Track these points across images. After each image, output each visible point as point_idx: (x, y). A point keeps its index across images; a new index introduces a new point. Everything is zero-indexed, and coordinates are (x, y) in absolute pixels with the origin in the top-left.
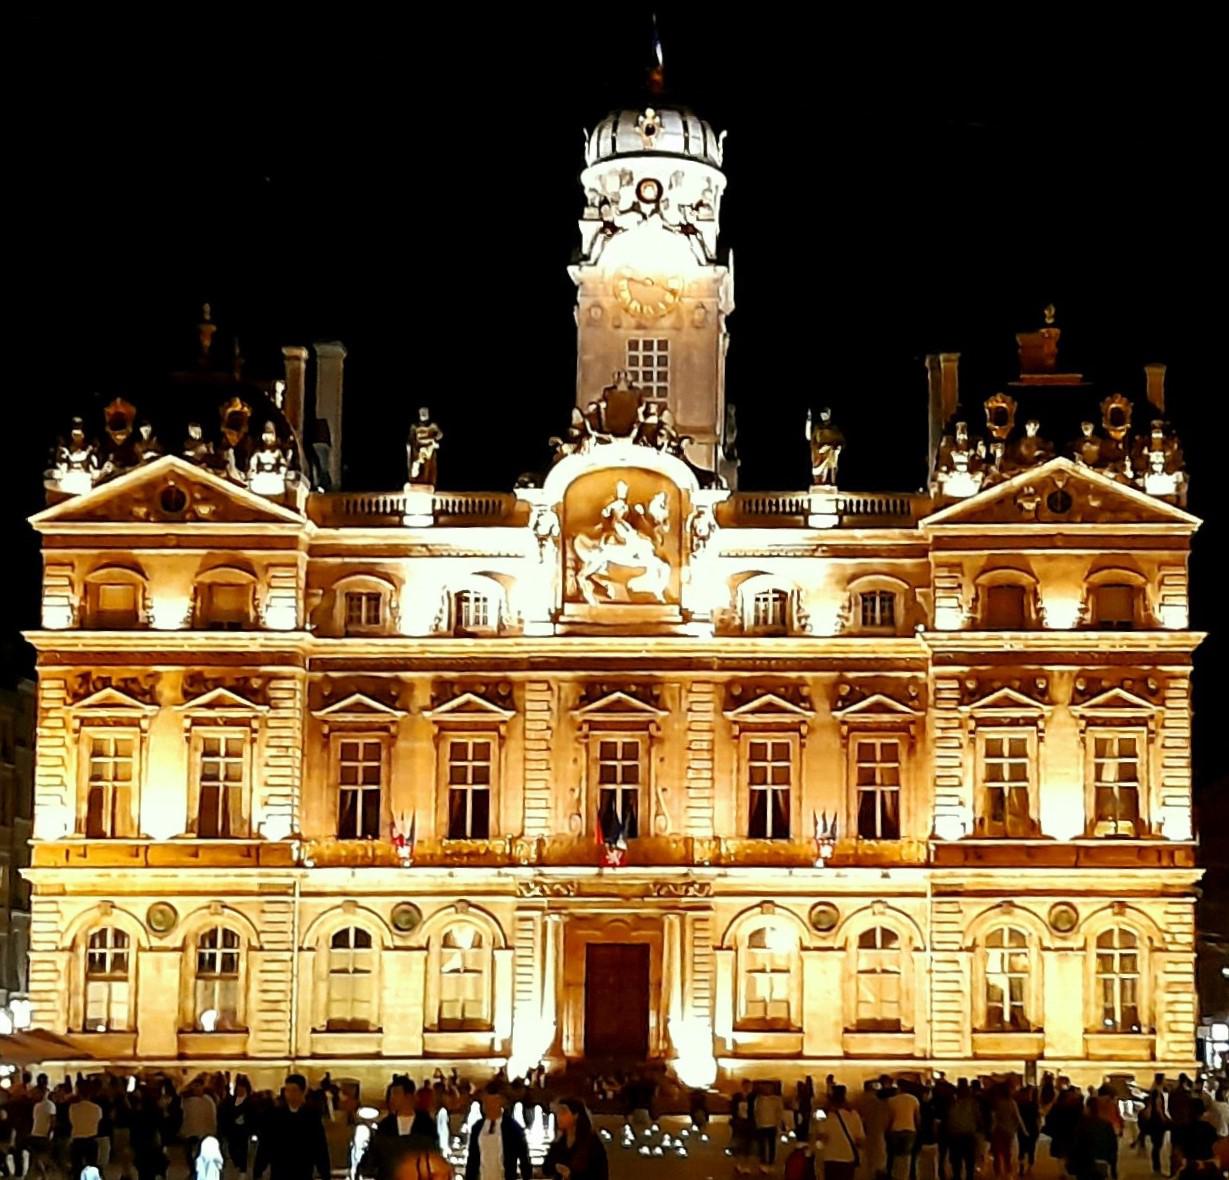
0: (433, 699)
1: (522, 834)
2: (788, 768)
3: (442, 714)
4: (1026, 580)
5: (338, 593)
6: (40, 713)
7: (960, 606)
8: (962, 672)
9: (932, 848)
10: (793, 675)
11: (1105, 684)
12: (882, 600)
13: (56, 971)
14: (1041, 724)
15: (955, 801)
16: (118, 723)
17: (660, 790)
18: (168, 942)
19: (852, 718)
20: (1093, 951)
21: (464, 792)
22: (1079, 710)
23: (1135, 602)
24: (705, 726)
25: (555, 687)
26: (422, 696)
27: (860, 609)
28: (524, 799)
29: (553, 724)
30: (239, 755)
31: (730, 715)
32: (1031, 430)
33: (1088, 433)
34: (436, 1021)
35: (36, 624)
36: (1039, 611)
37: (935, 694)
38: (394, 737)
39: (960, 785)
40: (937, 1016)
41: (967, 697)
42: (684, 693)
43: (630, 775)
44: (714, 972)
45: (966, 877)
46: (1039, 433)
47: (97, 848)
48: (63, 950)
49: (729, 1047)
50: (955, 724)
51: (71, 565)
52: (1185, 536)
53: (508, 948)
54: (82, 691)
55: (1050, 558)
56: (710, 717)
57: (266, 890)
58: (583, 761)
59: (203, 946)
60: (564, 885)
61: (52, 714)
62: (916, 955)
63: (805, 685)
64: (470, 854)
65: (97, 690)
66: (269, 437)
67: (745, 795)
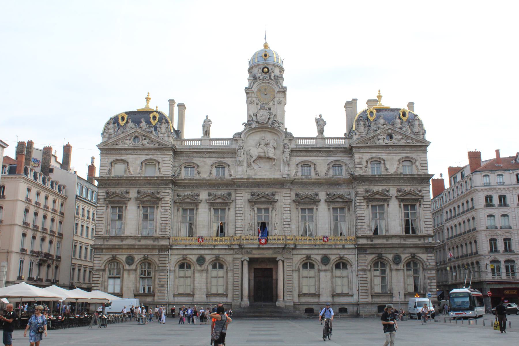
24: (288, 203)
40: (360, 288)
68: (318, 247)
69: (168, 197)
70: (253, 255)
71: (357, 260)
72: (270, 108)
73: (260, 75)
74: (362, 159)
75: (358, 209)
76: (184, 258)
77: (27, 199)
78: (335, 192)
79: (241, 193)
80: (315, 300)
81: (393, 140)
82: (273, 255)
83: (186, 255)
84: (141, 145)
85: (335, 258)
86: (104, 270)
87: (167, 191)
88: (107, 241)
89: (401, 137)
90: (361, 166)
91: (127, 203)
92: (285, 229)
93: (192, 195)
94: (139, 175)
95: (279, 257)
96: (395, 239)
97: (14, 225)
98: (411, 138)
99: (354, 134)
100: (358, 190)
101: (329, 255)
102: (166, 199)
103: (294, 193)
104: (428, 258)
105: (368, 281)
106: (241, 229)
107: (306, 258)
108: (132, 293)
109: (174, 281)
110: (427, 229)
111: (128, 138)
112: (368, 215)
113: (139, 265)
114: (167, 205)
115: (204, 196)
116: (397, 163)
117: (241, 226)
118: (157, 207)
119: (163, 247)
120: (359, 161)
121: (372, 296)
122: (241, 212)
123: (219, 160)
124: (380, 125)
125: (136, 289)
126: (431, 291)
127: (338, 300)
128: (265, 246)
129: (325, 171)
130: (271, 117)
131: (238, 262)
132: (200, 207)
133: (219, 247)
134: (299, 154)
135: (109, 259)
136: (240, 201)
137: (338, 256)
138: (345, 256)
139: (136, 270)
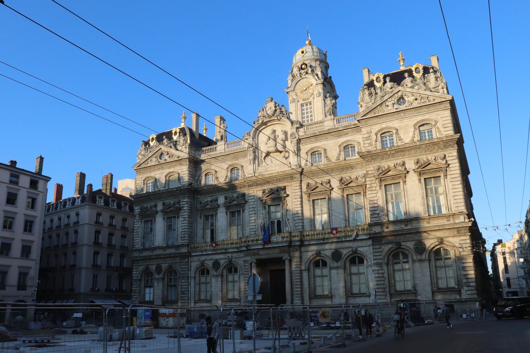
68: (327, 241)
69: (186, 205)
70: (259, 256)
72: (310, 103)
73: (297, 72)
74: (371, 132)
76: (203, 263)
77: (97, 222)
78: (348, 176)
79: (253, 192)
80: (328, 302)
81: (406, 104)
82: (280, 254)
83: (204, 261)
84: (164, 160)
85: (347, 253)
86: (140, 280)
87: (186, 200)
88: (142, 253)
89: (413, 98)
90: (369, 141)
91: (155, 216)
92: (297, 225)
93: (211, 201)
94: (164, 189)
95: (285, 256)
96: (416, 223)
97: (83, 245)
98: (427, 96)
99: (359, 106)
100: (368, 169)
101: (340, 250)
102: (185, 208)
103: (305, 184)
104: (461, 242)
105: (385, 278)
106: (254, 230)
107: (315, 255)
108: (161, 300)
109: (195, 288)
110: (457, 206)
111: (154, 156)
112: (381, 198)
113: (166, 274)
114: (186, 213)
115: (221, 200)
116: (413, 130)
117: (254, 227)
118: (178, 217)
119: (182, 255)
120: (367, 136)
121: (391, 295)
122: (254, 212)
123: (234, 162)
124: (388, 90)
127: (352, 301)
128: (270, 246)
129: (337, 155)
130: (277, 109)
131: (247, 264)
132: (218, 212)
133: (230, 251)
134: (309, 140)
135: (143, 270)
136: (252, 200)
137: (350, 249)
138: (359, 249)
139: (163, 279)
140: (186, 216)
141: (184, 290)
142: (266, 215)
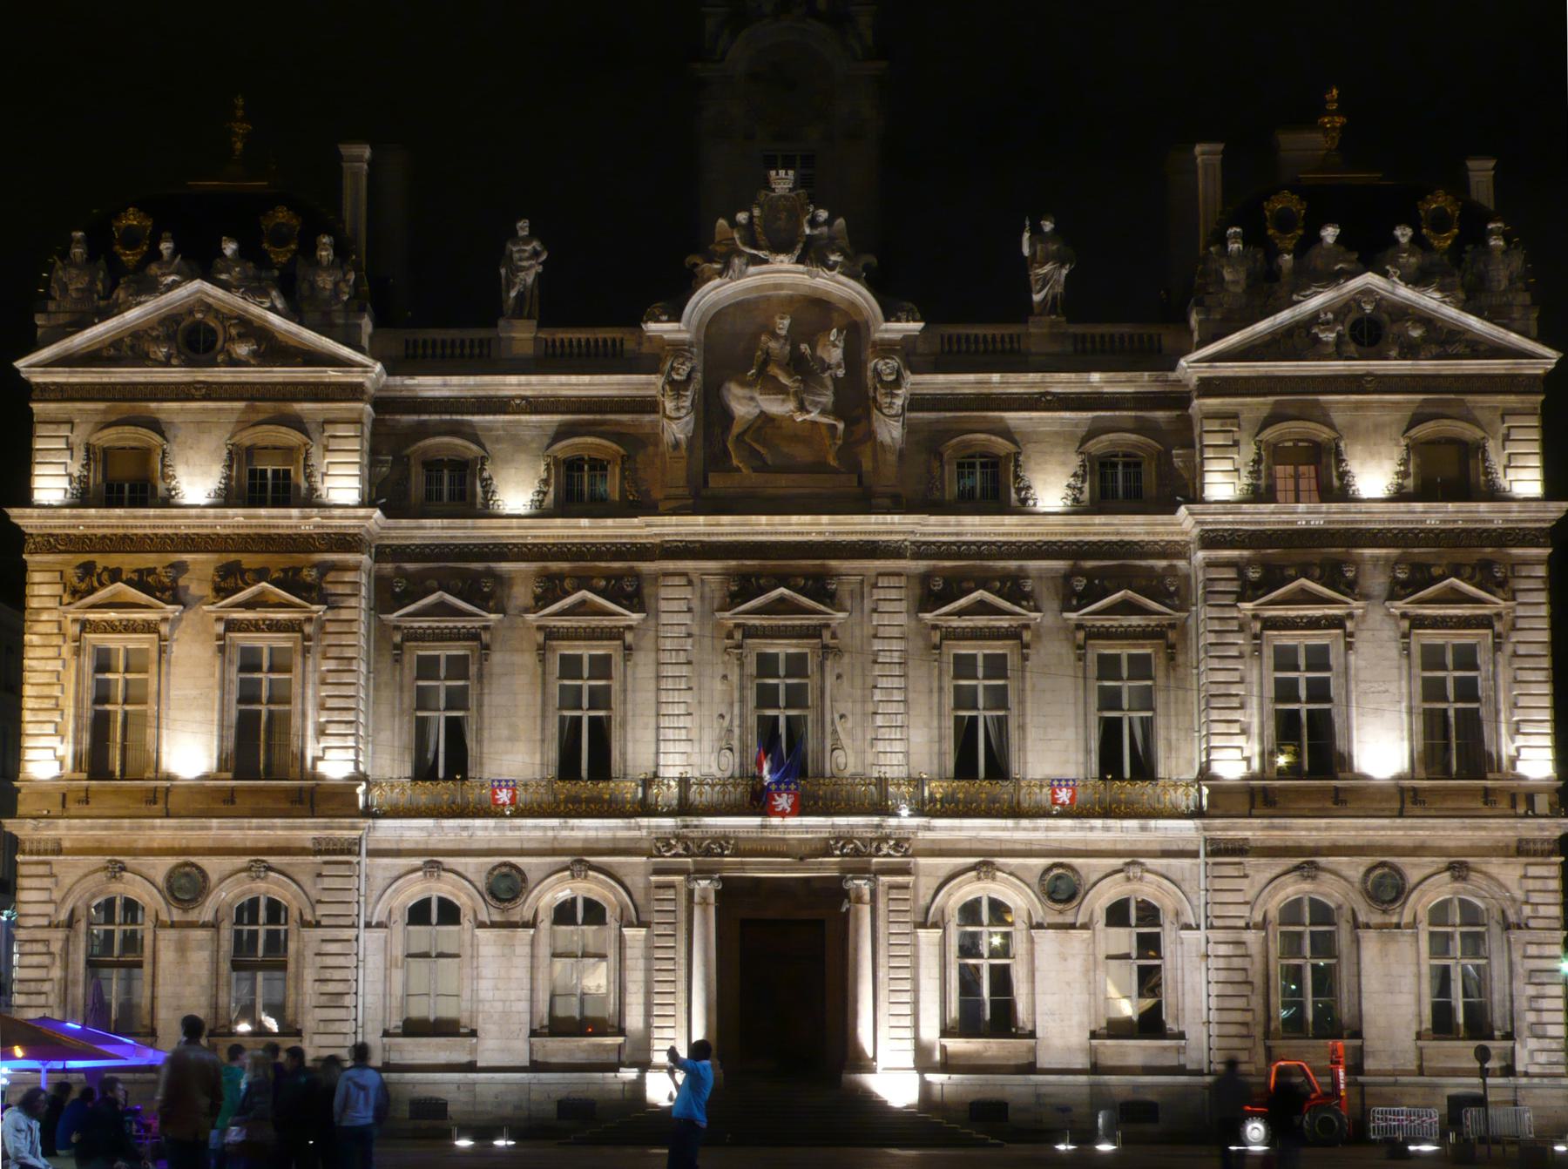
0: (537, 598)
1: (656, 775)
2: (1005, 687)
3: (548, 616)
4: (1324, 434)
5: (412, 462)
6: (27, 616)
7: (1237, 470)
8: (1241, 557)
9: (1205, 791)
10: (1013, 564)
11: (1436, 571)
12: (1126, 465)
13: (49, 953)
14: (1349, 625)
15: (1235, 728)
16: (129, 627)
17: (836, 717)
18: (192, 916)
19: (1090, 621)
20: (1424, 930)
21: (579, 719)
22: (1398, 607)
23: (1472, 463)
24: (895, 632)
25: (696, 580)
26: (521, 594)
27: (1097, 478)
28: (658, 728)
29: (695, 630)
30: (288, 670)
31: (928, 617)
32: (1330, 234)
33: (1404, 240)
34: (546, 1022)
35: (25, 499)
36: (1343, 475)
37: (1204, 588)
38: (487, 647)
39: (1242, 707)
41: (1249, 591)
42: (866, 589)
43: (796, 697)
44: (915, 957)
45: (1251, 830)
46: (1339, 240)
47: (99, 792)
48: (57, 926)
49: (937, 1056)
50: (1234, 625)
51: (71, 423)
52: (1537, 376)
53: (641, 924)
54: (83, 586)
55: (1358, 406)
56: (902, 619)
57: (323, 847)
58: (734, 678)
59: (239, 921)
60: (715, 840)
61: (44, 617)
62: (1185, 934)
63: (1028, 577)
64: (588, 801)
65: (102, 585)
66: (325, 254)
67: (950, 724)
71: (1202, 887)
75: (1216, 664)
104: (1531, 884)
109: (387, 979)
125: (216, 1013)
126: (1540, 1033)
140: (349, 653)
141: (340, 988)
142: (742, 688)
